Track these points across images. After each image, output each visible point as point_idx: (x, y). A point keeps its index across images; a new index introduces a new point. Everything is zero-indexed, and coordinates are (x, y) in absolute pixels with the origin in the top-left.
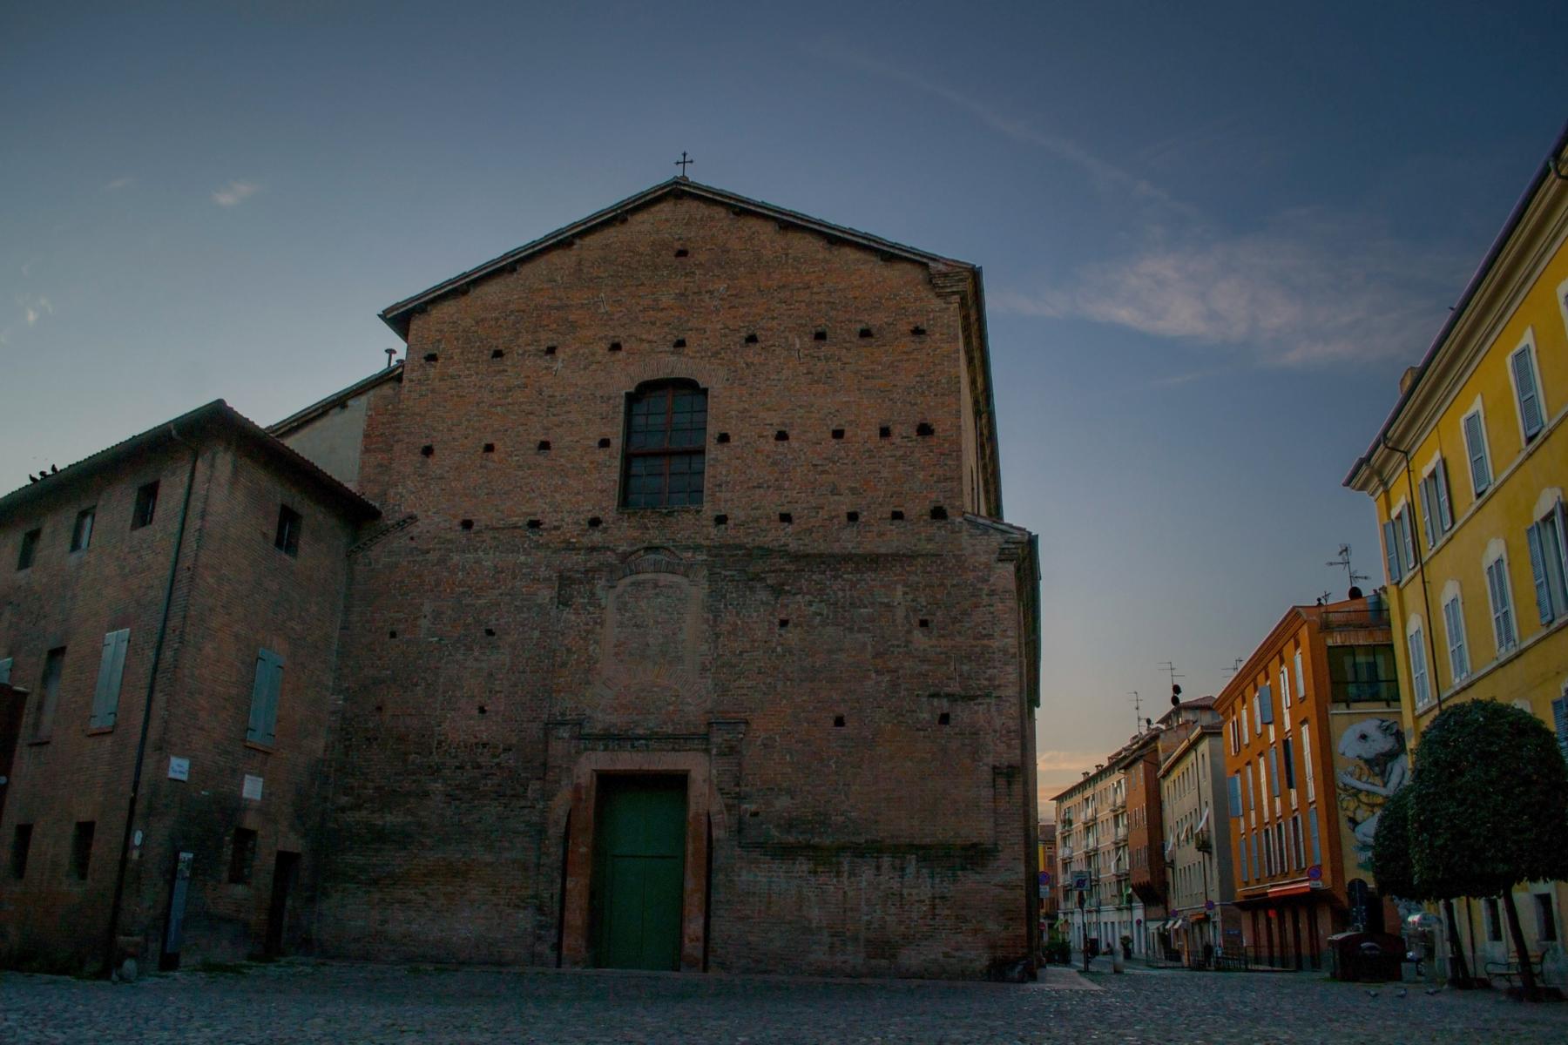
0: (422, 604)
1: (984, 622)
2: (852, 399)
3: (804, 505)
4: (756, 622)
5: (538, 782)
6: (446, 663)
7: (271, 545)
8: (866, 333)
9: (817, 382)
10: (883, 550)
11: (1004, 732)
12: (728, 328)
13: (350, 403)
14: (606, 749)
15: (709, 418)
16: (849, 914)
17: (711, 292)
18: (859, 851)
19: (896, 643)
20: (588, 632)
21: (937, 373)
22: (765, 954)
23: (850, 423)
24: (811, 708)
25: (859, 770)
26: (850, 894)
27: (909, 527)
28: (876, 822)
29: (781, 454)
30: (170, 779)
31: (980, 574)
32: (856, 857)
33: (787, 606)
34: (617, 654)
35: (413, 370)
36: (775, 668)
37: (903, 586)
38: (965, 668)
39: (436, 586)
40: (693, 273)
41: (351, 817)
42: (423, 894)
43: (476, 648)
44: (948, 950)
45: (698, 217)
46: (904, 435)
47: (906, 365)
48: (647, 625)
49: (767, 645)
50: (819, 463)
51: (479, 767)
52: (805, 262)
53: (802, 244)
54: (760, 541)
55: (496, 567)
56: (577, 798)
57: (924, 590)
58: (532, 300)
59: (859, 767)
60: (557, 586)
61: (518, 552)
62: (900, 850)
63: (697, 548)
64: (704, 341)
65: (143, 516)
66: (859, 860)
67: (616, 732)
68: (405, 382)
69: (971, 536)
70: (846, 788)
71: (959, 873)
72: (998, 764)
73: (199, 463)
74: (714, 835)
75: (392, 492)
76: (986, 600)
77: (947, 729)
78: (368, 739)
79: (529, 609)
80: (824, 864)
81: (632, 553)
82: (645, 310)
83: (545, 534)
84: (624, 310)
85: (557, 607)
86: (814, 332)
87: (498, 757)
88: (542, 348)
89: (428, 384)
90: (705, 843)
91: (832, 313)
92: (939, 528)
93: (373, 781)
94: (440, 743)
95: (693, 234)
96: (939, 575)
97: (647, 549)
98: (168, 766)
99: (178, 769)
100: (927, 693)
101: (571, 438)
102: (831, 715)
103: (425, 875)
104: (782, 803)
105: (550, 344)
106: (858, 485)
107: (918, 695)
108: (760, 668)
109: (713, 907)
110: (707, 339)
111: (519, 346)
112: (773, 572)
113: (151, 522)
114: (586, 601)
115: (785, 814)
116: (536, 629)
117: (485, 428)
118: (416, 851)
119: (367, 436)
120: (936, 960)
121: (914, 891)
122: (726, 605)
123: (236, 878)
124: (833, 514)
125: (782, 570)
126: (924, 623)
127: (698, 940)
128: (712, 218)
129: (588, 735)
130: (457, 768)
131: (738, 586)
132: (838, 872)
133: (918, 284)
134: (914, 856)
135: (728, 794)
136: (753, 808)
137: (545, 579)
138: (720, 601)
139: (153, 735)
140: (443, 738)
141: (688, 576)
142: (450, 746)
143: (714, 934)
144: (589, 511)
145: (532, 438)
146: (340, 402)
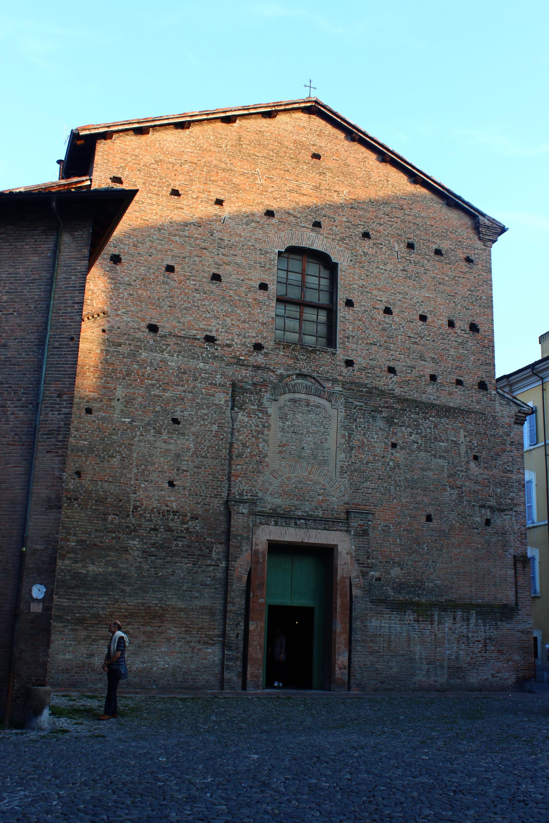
1: (508, 462)
3: (404, 364)
4: (376, 442)
6: (139, 441)
8: (438, 252)
10: (452, 405)
11: (519, 534)
12: (351, 223)
14: (276, 524)
16: (438, 649)
20: (258, 432)
22: (388, 677)
23: (431, 312)
24: (412, 507)
26: (439, 636)
29: (387, 324)
31: (506, 430)
32: (443, 611)
33: (396, 434)
34: (280, 452)
37: (465, 431)
38: (499, 490)
39: (127, 375)
43: (164, 432)
44: (493, 672)
45: (327, 133)
47: (463, 281)
48: (302, 433)
51: (170, 530)
54: (376, 383)
55: (179, 367)
57: (475, 435)
59: (441, 550)
60: (230, 392)
61: (198, 359)
62: (467, 607)
63: (335, 381)
64: (334, 228)
66: (443, 613)
67: (282, 512)
74: (353, 593)
76: (508, 448)
77: (489, 529)
78: (70, 499)
79: (208, 407)
80: (423, 615)
81: (288, 376)
82: (290, 191)
83: (219, 349)
84: (275, 186)
85: (232, 409)
87: (187, 524)
88: (211, 198)
90: (348, 599)
91: (418, 232)
92: (483, 395)
93: (75, 535)
94: (136, 507)
97: (298, 375)
100: (479, 504)
102: (424, 513)
103: (126, 617)
104: (395, 572)
106: (436, 357)
107: (473, 505)
109: (353, 644)
110: (336, 226)
112: (387, 407)
114: (256, 407)
115: (398, 580)
116: (215, 424)
117: (166, 252)
120: (487, 679)
124: (421, 373)
125: (393, 408)
126: (476, 458)
127: (345, 668)
128: (337, 138)
130: (152, 529)
131: (364, 414)
132: (431, 621)
134: (474, 611)
136: (377, 574)
140: (138, 504)
141: (330, 401)
143: (355, 664)
144: (254, 337)
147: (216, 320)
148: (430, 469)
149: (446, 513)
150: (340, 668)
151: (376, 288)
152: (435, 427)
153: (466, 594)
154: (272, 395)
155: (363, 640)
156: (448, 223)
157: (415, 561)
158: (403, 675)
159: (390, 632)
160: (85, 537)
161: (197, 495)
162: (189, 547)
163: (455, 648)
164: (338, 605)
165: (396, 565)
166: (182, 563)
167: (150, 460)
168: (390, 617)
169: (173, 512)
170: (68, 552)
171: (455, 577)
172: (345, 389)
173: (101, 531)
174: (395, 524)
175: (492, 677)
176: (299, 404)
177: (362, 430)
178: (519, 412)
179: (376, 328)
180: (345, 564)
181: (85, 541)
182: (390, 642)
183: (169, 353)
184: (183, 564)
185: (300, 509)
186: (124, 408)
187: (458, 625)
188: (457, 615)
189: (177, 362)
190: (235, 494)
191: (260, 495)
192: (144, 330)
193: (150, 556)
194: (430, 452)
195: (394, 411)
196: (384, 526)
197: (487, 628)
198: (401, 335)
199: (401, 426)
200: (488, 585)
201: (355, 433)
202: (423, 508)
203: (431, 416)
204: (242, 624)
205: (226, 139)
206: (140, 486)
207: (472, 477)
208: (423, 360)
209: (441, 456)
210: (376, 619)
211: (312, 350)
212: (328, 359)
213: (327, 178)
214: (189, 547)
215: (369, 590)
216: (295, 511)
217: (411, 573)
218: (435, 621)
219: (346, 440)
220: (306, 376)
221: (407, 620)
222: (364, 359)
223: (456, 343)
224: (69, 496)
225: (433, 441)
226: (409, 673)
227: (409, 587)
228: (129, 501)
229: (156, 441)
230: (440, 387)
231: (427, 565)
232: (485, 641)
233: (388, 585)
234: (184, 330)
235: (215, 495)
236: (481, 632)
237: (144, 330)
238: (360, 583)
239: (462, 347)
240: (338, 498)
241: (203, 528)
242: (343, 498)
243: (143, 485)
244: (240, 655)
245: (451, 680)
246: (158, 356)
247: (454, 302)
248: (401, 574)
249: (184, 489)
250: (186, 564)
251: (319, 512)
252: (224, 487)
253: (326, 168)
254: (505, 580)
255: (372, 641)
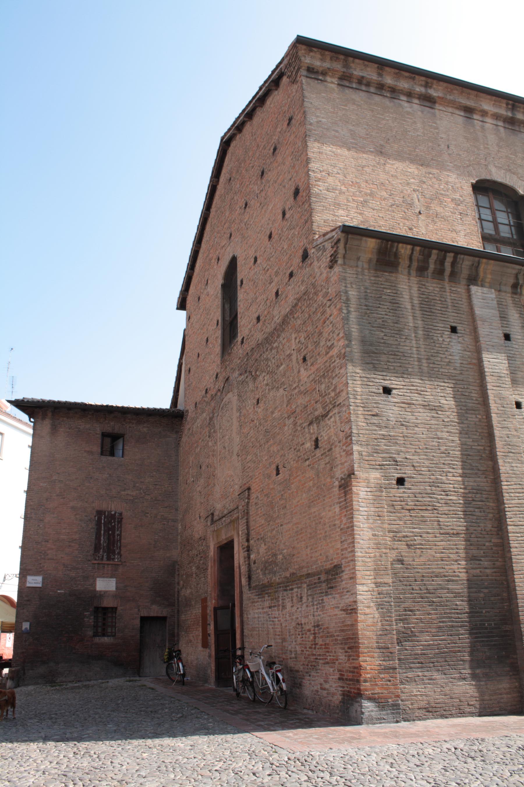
99: (33, 582)
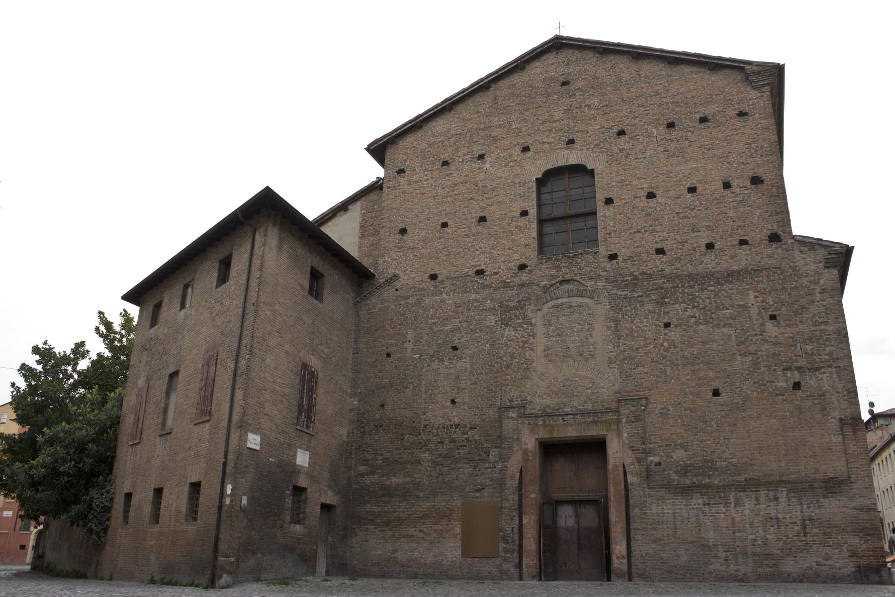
0: (407, 333)
1: (820, 313)
2: (700, 165)
3: (674, 241)
4: (647, 326)
5: (497, 449)
6: (427, 371)
7: (306, 293)
8: (703, 120)
9: (672, 156)
10: (735, 268)
11: (845, 393)
12: (604, 128)
13: (350, 207)
15: (597, 189)
16: (738, 534)
17: (589, 106)
18: (743, 488)
19: (753, 333)
20: (524, 342)
21: (761, 140)
23: (700, 182)
25: (735, 427)
26: (737, 519)
27: (753, 250)
28: (752, 465)
29: (652, 207)
30: (248, 448)
31: (812, 278)
33: (668, 313)
34: (546, 356)
35: (389, 181)
36: (664, 358)
38: (809, 347)
39: (415, 320)
40: (574, 95)
41: (368, 480)
42: (420, 531)
43: (445, 359)
46: (741, 185)
48: (567, 335)
49: (656, 342)
50: (681, 211)
51: (454, 441)
52: (654, 78)
53: (648, 68)
55: (455, 303)
56: (526, 460)
58: (465, 126)
59: (735, 425)
62: (773, 484)
64: (588, 138)
65: (223, 278)
66: (742, 494)
67: (550, 411)
68: (385, 189)
69: (801, 252)
70: (727, 441)
71: (822, 500)
72: (843, 417)
73: (257, 235)
74: (629, 481)
75: (381, 261)
76: (818, 297)
77: (799, 393)
78: (377, 427)
79: (481, 330)
80: (715, 498)
81: (551, 286)
82: (543, 123)
84: (528, 124)
86: (666, 123)
87: (467, 434)
89: (400, 189)
90: (623, 486)
91: (678, 109)
93: (381, 455)
94: (425, 426)
95: (571, 70)
96: (780, 281)
98: (247, 439)
100: (782, 367)
101: (501, 212)
102: (709, 388)
103: (421, 518)
104: (679, 454)
105: (480, 153)
106: (711, 224)
108: (652, 359)
109: (632, 533)
110: (590, 136)
111: (459, 157)
113: (228, 281)
114: (521, 321)
115: (682, 463)
117: (440, 213)
118: (413, 502)
119: (362, 227)
120: (811, 568)
121: (788, 516)
122: (623, 316)
123: (297, 520)
124: (695, 245)
126: (773, 317)
127: (623, 557)
129: (530, 414)
130: (438, 443)
132: (726, 504)
133: (737, 83)
134: (784, 489)
135: (637, 450)
136: (657, 459)
137: (491, 309)
138: (618, 313)
139: (235, 418)
140: (427, 423)
142: (432, 428)
144: (518, 260)
145: (473, 215)
146: (343, 207)
147: (484, 255)
148: (713, 341)
149: (738, 384)
150: (618, 558)
151: (635, 178)
152: (716, 295)
153: (773, 470)
154: (536, 306)
155: (644, 528)
156: (712, 87)
157: (702, 441)
158: (695, 563)
159: (674, 519)
160: (388, 455)
161: (474, 407)
162: (470, 453)
163: (761, 532)
164: (612, 494)
165: (679, 448)
166: (464, 468)
167: (435, 385)
168: (674, 502)
169: (455, 425)
170: (377, 469)
171: (756, 452)
172: (608, 282)
173: (399, 449)
174: (675, 404)
175: (817, 565)
176: (561, 308)
177: (629, 317)
178: (830, 254)
179: (639, 216)
180: (617, 452)
181: (388, 459)
182: (675, 529)
183: (446, 293)
184: (466, 469)
185: (569, 405)
186: (414, 347)
187: (761, 507)
188: (760, 494)
189: (453, 299)
190: (505, 401)
191: (529, 398)
192: (427, 280)
193: (438, 465)
194: (712, 323)
195: (665, 291)
196: (662, 409)
197: (805, 507)
198: (668, 214)
199: (673, 304)
200: (804, 457)
201: (621, 322)
202: (707, 383)
203: (710, 285)
204: (517, 518)
205: (484, 104)
206: (428, 407)
207: (769, 339)
208: (696, 232)
209: (726, 324)
210: (658, 506)
211: (575, 255)
212: (591, 259)
213: (578, 97)
214: (470, 453)
215: (648, 475)
216: (564, 408)
217: (698, 453)
218: (730, 503)
219: (612, 331)
220: (569, 281)
221: (695, 505)
222: (628, 249)
223: (736, 203)
224: (376, 424)
225: (714, 311)
226: (701, 562)
227: (697, 469)
228: (420, 422)
229: (439, 368)
230: (720, 252)
231: (718, 443)
232: (804, 523)
233: (670, 469)
234: (458, 271)
235: (490, 405)
236: (796, 512)
237: (427, 280)
238: (636, 470)
239: (743, 205)
240: (608, 389)
241: (480, 436)
242: (613, 388)
243: (430, 407)
244: (516, 547)
245: (759, 569)
246: (438, 298)
247: (728, 163)
248: (686, 456)
249: (464, 404)
250: (468, 468)
251: (589, 406)
252: (497, 397)
253: (575, 90)
254: (829, 449)
255: (654, 528)
